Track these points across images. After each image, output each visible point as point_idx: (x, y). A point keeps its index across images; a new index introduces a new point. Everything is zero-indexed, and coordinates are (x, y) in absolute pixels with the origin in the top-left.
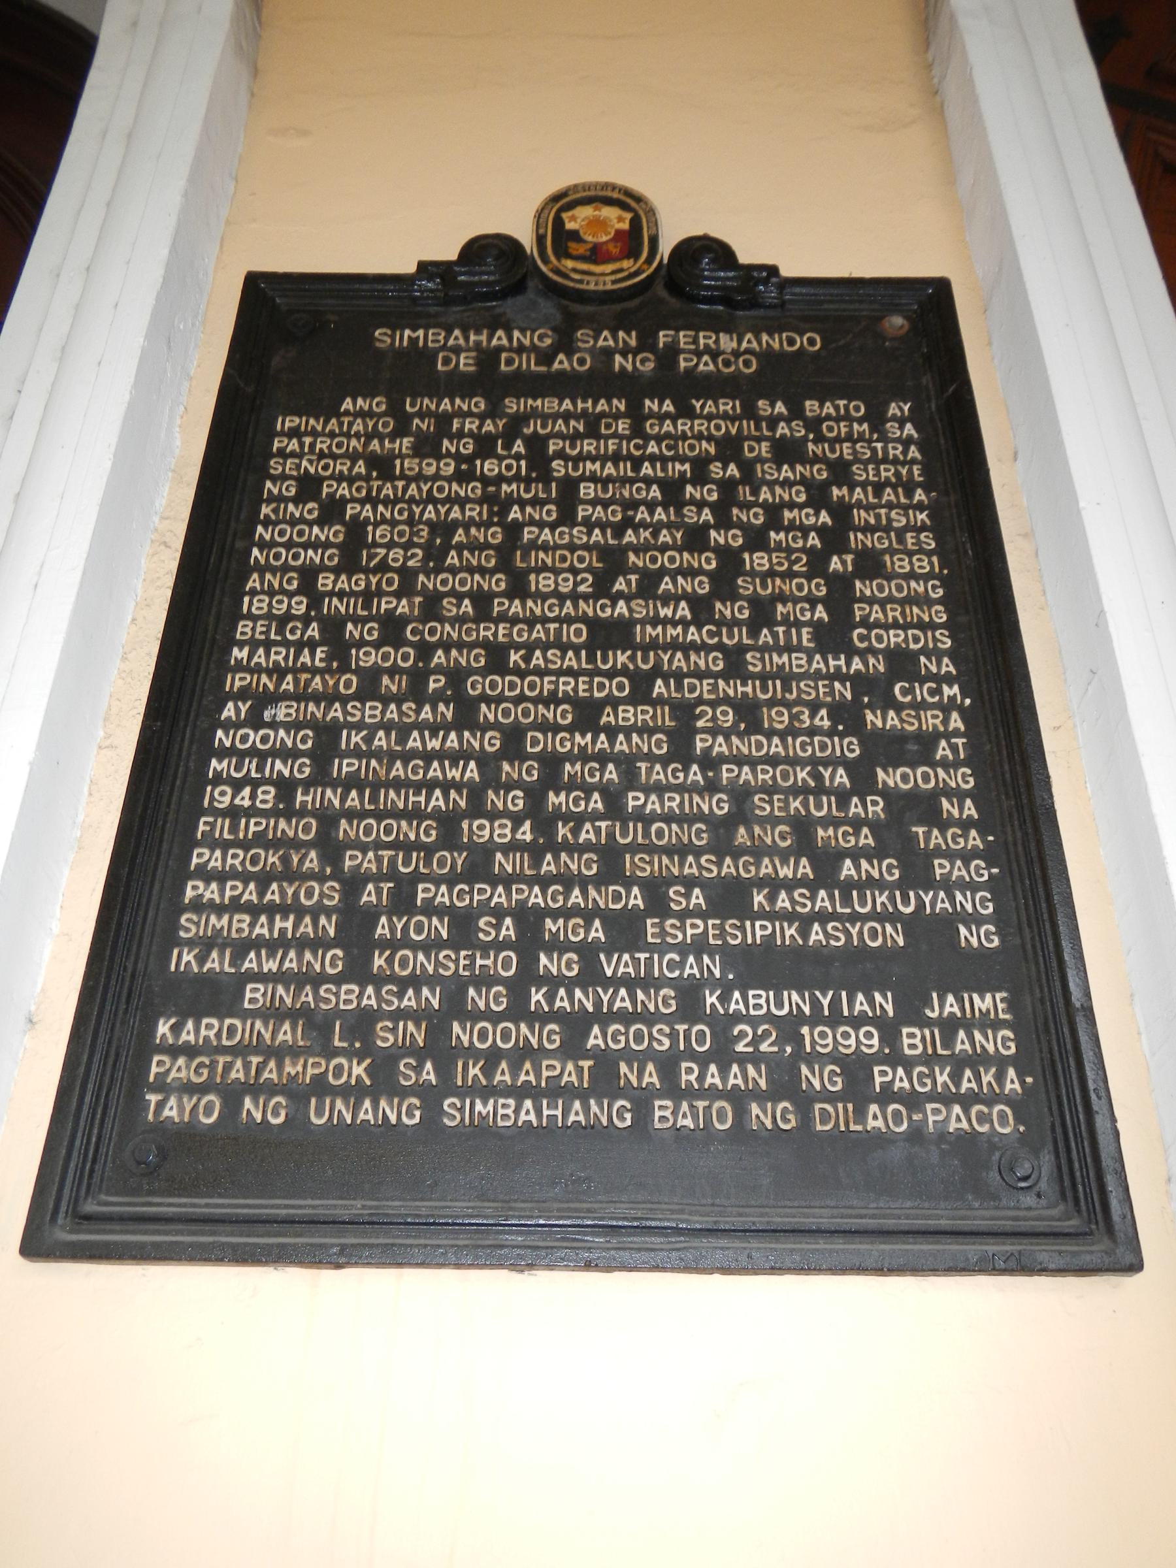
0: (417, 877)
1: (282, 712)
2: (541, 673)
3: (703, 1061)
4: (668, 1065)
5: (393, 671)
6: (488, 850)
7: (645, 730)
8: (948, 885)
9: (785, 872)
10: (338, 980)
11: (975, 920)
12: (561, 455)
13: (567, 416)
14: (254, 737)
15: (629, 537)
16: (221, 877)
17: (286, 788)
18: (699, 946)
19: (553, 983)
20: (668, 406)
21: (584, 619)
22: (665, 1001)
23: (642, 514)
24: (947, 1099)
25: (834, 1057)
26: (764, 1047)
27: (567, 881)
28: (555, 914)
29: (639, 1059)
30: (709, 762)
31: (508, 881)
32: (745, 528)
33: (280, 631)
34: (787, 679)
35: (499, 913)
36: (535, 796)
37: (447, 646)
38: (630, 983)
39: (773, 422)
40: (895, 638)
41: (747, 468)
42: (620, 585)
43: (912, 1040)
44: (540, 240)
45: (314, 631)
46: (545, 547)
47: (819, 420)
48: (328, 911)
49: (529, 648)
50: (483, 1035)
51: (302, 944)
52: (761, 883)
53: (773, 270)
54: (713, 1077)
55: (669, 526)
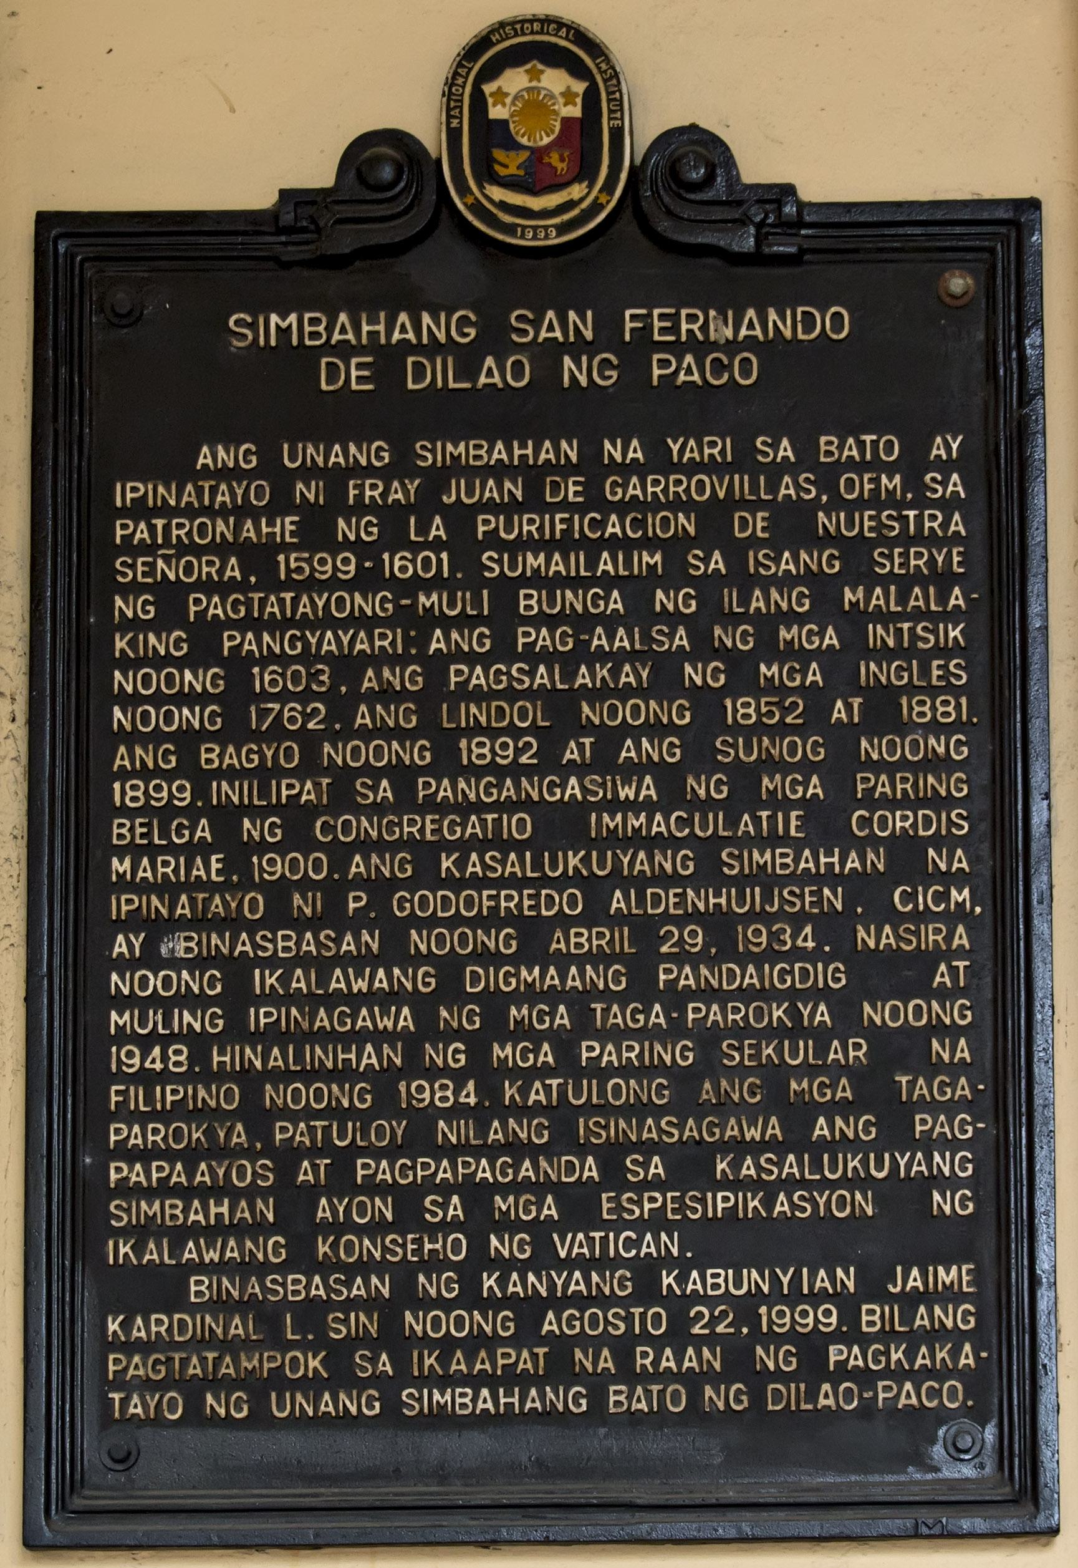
0: (354, 1151)
1: (178, 946)
2: (479, 883)
3: (657, 1344)
4: (623, 1348)
5: (305, 885)
6: (432, 1114)
7: (599, 958)
8: (928, 1144)
9: (753, 1134)
10: (283, 1268)
11: (951, 1183)
12: (493, 540)
13: (500, 471)
14: (155, 982)
15: (583, 678)
16: (145, 1155)
17: (199, 1044)
18: (657, 1222)
19: (505, 1266)
20: (636, 452)
21: (526, 804)
22: (620, 1284)
23: (599, 640)
24: (899, 1375)
25: (793, 1336)
26: (720, 1329)
27: (517, 1149)
28: (504, 1190)
29: (598, 1344)
30: (676, 999)
31: (452, 1152)
32: (730, 657)
33: (164, 833)
34: (767, 880)
35: (446, 1190)
36: (478, 1046)
37: (365, 846)
38: (586, 1265)
39: (776, 471)
40: (899, 822)
41: (736, 552)
42: (571, 754)
43: (871, 1316)
44: (454, 136)
45: (204, 831)
46: (479, 696)
47: (838, 467)
48: (264, 1193)
49: (464, 847)
50: (436, 1323)
51: (239, 1230)
52: (724, 1147)
53: (788, 190)
54: (668, 1362)
55: (632, 656)
